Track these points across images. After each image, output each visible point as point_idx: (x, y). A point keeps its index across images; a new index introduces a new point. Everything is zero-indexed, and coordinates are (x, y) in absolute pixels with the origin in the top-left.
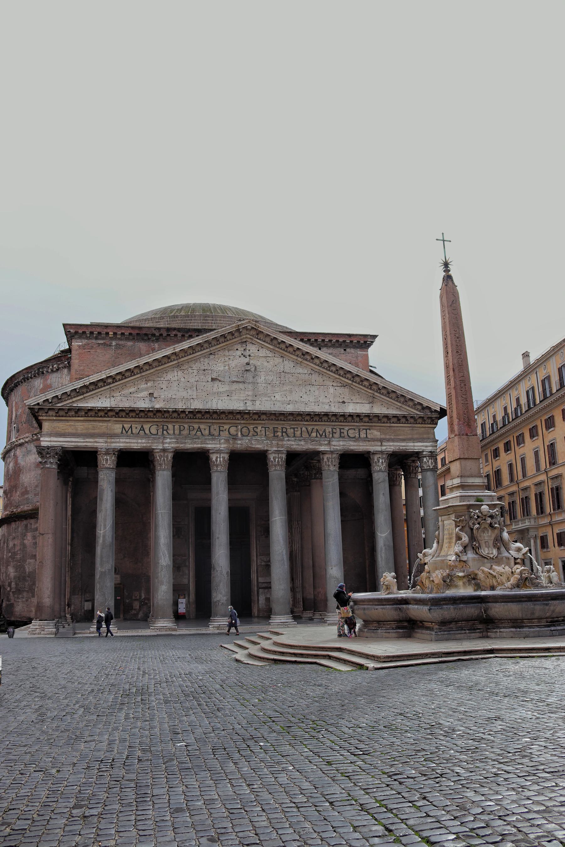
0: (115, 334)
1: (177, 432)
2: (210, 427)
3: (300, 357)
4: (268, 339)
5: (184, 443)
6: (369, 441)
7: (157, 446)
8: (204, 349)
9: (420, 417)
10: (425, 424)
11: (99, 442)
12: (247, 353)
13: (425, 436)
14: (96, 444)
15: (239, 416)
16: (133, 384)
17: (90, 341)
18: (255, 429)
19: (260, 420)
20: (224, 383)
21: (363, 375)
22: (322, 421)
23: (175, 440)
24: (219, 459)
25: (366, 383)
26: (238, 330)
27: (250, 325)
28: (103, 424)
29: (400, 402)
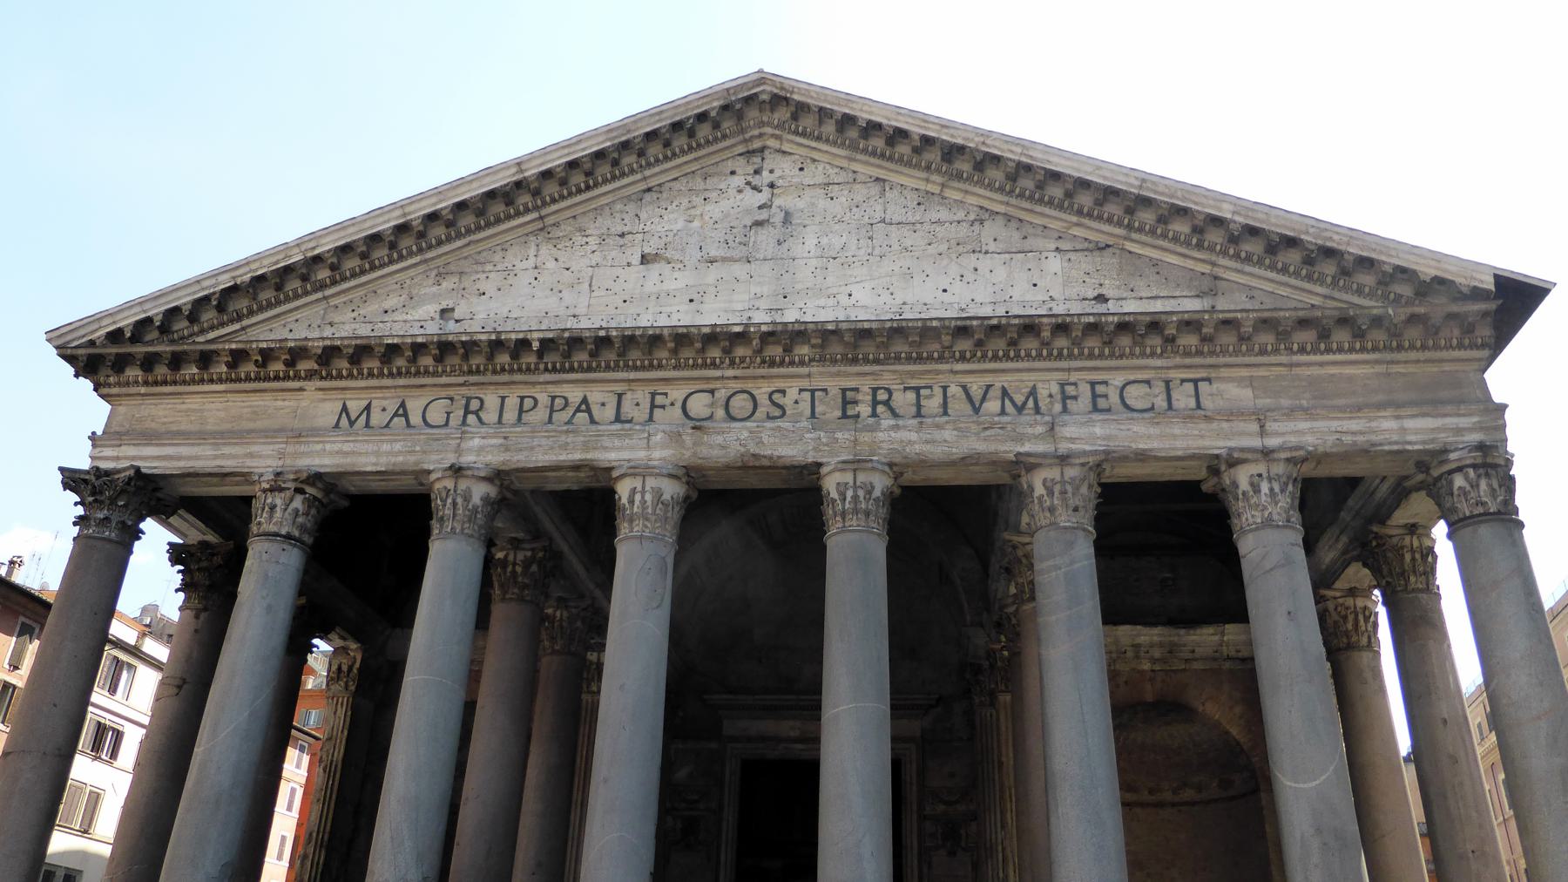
1: (510, 415)
2: (620, 396)
3: (938, 171)
6: (1208, 419)
7: (436, 461)
8: (623, 175)
9: (1413, 319)
10: (1436, 347)
11: (260, 457)
14: (249, 463)
15: (715, 353)
19: (792, 363)
20: (681, 266)
22: (1018, 357)
23: (501, 441)
24: (638, 497)
25: (1181, 227)
26: (725, 108)
28: (287, 403)
29: (1321, 281)
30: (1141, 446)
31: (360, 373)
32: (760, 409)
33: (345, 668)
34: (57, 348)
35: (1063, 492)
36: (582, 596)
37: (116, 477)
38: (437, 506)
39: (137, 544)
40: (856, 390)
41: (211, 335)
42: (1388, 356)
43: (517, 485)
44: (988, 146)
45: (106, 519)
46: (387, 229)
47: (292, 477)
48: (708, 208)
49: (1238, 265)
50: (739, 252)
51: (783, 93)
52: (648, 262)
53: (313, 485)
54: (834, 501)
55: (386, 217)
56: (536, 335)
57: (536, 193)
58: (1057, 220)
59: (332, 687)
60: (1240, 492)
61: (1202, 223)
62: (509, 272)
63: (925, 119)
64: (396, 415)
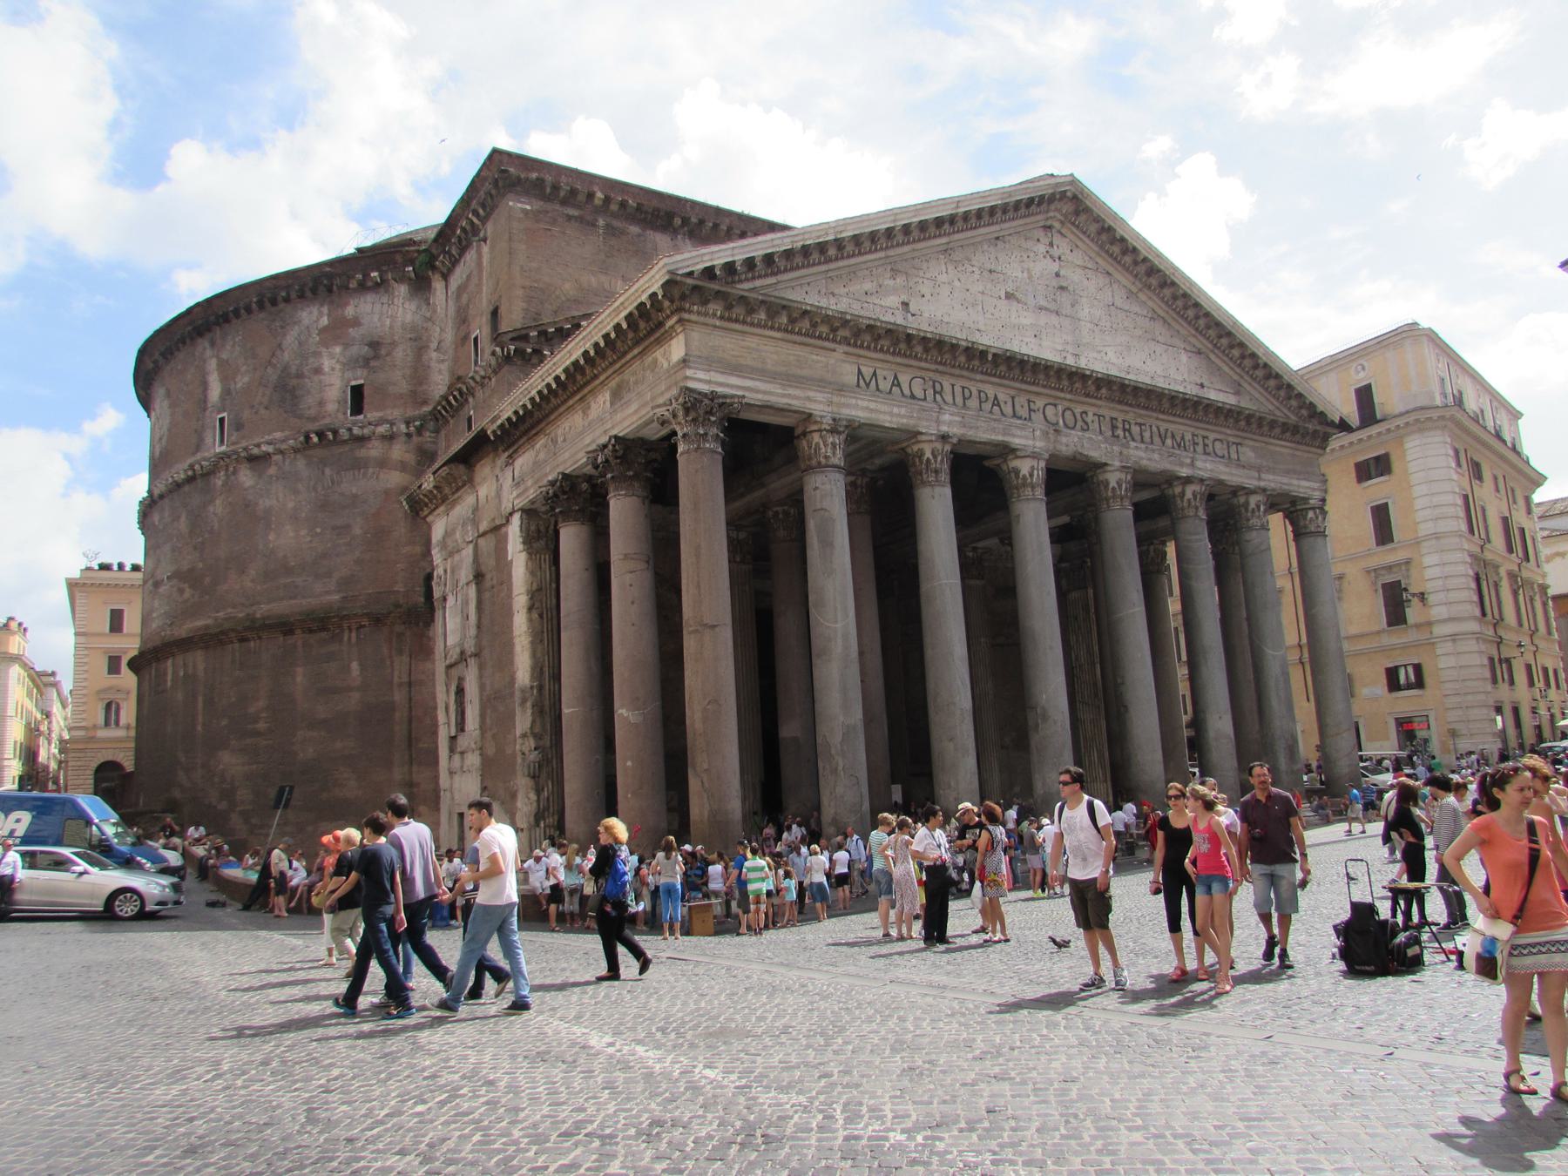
0: (607, 200)
1: (959, 400)
2: (1013, 398)
6: (1244, 467)
7: (928, 428)
12: (1055, 252)
16: (868, 272)
17: (549, 206)
19: (1096, 398)
30: (1223, 477)
31: (875, 348)
33: (542, 529)
38: (928, 459)
47: (845, 423)
48: (1032, 265)
49: (1249, 380)
50: (1052, 306)
54: (1113, 488)
56: (993, 350)
58: (1185, 330)
59: (535, 545)
63: (1150, 248)
64: (893, 385)
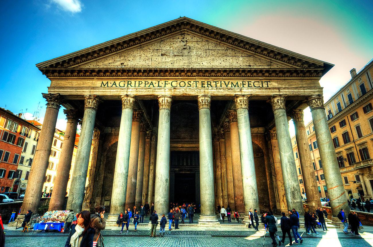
1: (137, 85)
3: (219, 40)
4: (198, 30)
5: (141, 92)
6: (270, 89)
7: (123, 93)
8: (157, 37)
9: (309, 71)
11: (86, 92)
12: (185, 39)
13: (312, 85)
14: (83, 93)
15: (178, 74)
18: (189, 83)
19: (192, 76)
20: (169, 56)
21: (263, 45)
22: (235, 76)
24: (163, 101)
27: (186, 21)
28: (90, 81)
29: (291, 64)
30: (257, 94)
32: (186, 85)
33: (97, 134)
34: (38, 68)
35: (243, 102)
36: (145, 121)
37: (55, 95)
39: (60, 109)
40: (204, 82)
41: (72, 67)
42: (303, 78)
43: (138, 99)
44: (230, 35)
45: (53, 104)
46: (109, 46)
50: (181, 54)
51: (189, 22)
52: (163, 55)
53: (97, 98)
54: (201, 103)
55: (109, 43)
56: (142, 69)
57: (139, 40)
60: (275, 103)
61: (269, 52)
62: (134, 56)
63: (217, 28)
64: (113, 84)
